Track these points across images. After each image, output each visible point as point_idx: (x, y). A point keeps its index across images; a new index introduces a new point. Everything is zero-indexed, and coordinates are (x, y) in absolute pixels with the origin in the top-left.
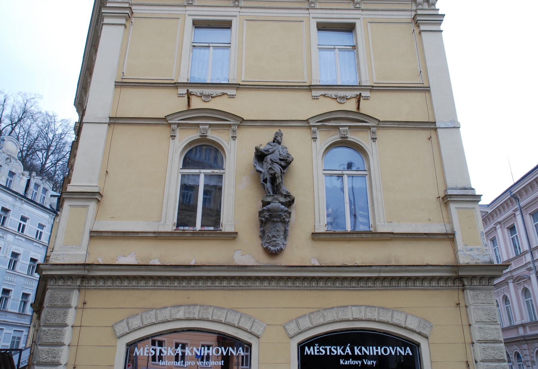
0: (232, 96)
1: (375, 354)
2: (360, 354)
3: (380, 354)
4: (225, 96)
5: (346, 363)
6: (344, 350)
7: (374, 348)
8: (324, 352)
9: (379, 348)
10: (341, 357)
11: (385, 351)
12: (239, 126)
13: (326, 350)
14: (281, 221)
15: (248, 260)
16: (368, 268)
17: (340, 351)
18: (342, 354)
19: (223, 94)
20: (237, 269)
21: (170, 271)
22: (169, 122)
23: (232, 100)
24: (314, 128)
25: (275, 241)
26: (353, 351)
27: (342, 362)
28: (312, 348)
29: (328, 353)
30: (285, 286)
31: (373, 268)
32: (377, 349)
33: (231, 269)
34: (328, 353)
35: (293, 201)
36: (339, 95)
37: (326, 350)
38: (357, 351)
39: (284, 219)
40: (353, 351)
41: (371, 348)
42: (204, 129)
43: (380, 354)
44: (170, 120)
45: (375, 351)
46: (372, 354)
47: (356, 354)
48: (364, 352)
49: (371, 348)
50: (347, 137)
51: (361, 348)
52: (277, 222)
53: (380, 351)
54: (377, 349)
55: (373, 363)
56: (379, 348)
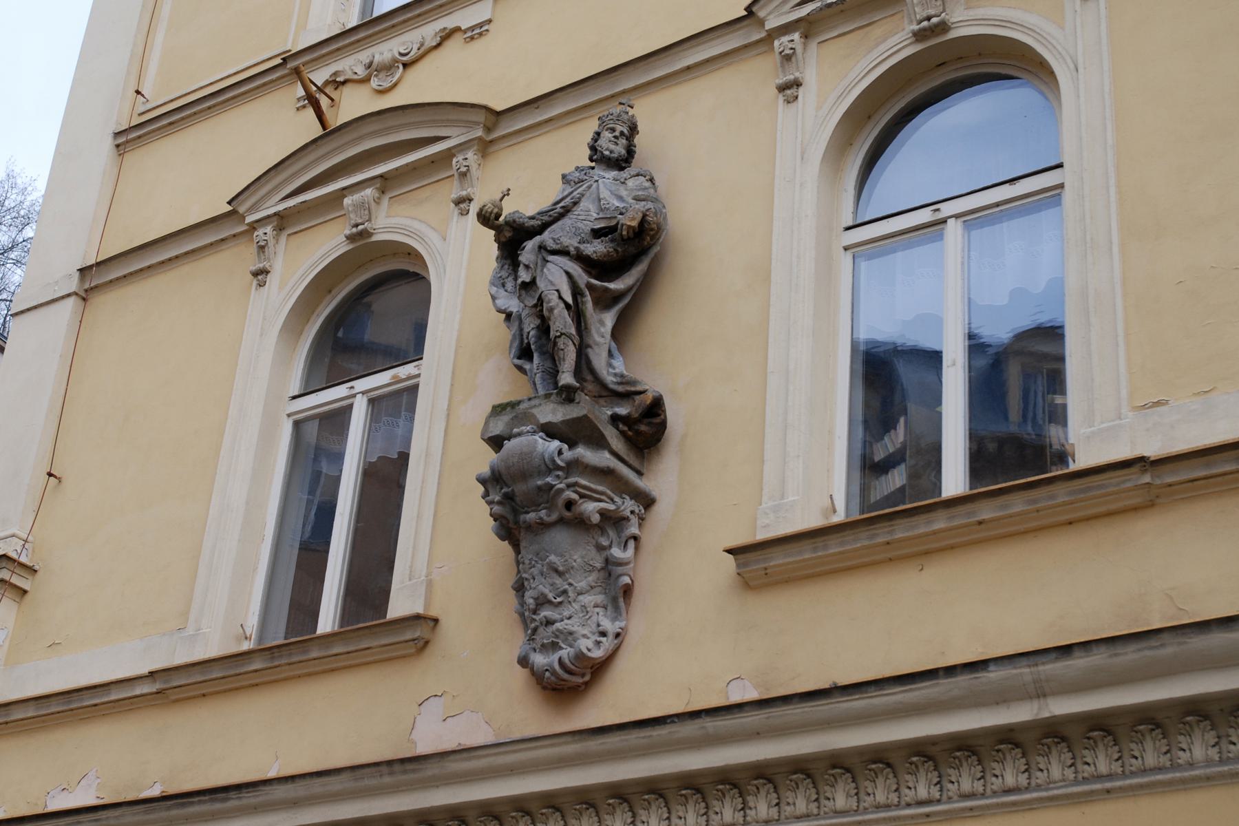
0: (478, 31)
4: (458, 39)
14: (561, 521)
16: (963, 680)
20: (387, 780)
23: (478, 45)
25: (549, 622)
31: (994, 675)
33: (367, 782)
35: (655, 408)
39: (569, 505)
52: (544, 526)
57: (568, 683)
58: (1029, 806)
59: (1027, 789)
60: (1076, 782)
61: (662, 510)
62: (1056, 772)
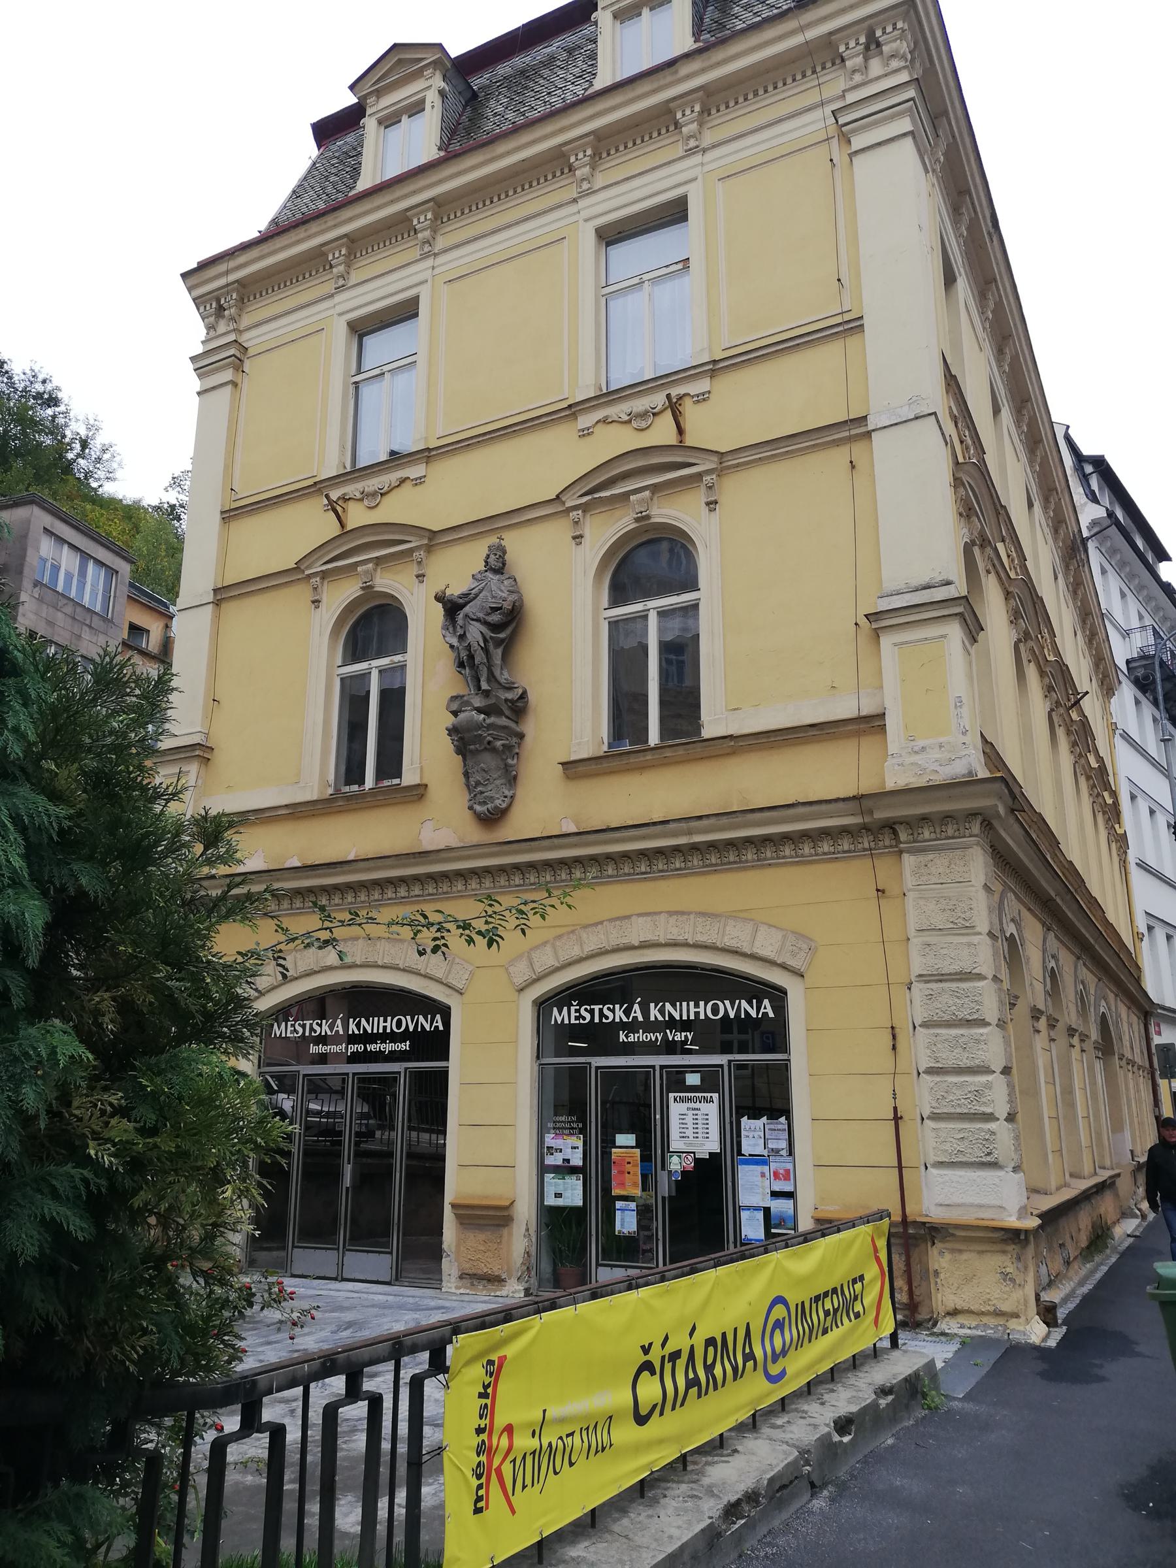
1: (692, 1017)
2: (660, 1018)
3: (702, 1017)
5: (631, 1039)
6: (627, 1012)
7: (692, 1004)
8: (588, 1016)
9: (702, 1003)
10: (623, 1026)
11: (715, 1010)
12: (429, 549)
13: (592, 1012)
15: (433, 837)
17: (620, 1014)
18: (625, 1019)
19: (403, 481)
21: (307, 877)
22: (307, 572)
24: (575, 513)
26: (646, 1012)
27: (622, 1037)
28: (565, 1009)
29: (597, 1020)
30: (510, 886)
32: (697, 1006)
34: (597, 1020)
36: (635, 410)
37: (592, 1012)
38: (654, 1013)
40: (646, 1012)
41: (684, 1004)
42: (366, 572)
43: (702, 1017)
44: (308, 568)
45: (692, 1010)
46: (685, 1017)
47: (652, 1019)
48: (670, 1014)
49: (684, 1004)
50: (648, 517)
51: (664, 1006)
53: (704, 1010)
54: (697, 1006)
55: (686, 1036)
56: (702, 1003)
57: (492, 818)
58: (686, 876)
59: (685, 869)
60: (704, 867)
61: (528, 739)
62: (695, 863)
